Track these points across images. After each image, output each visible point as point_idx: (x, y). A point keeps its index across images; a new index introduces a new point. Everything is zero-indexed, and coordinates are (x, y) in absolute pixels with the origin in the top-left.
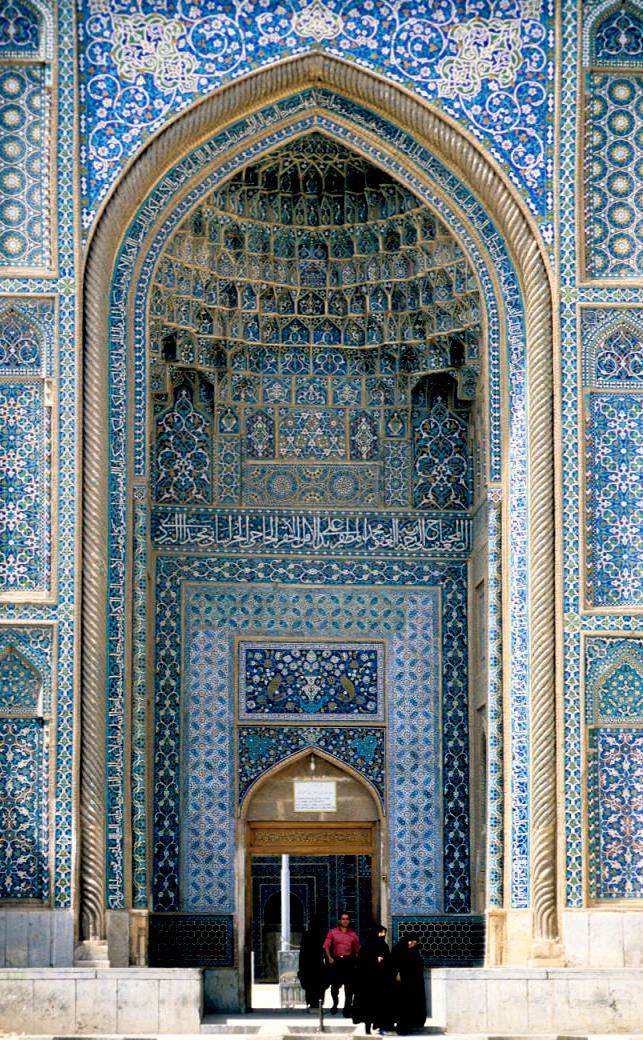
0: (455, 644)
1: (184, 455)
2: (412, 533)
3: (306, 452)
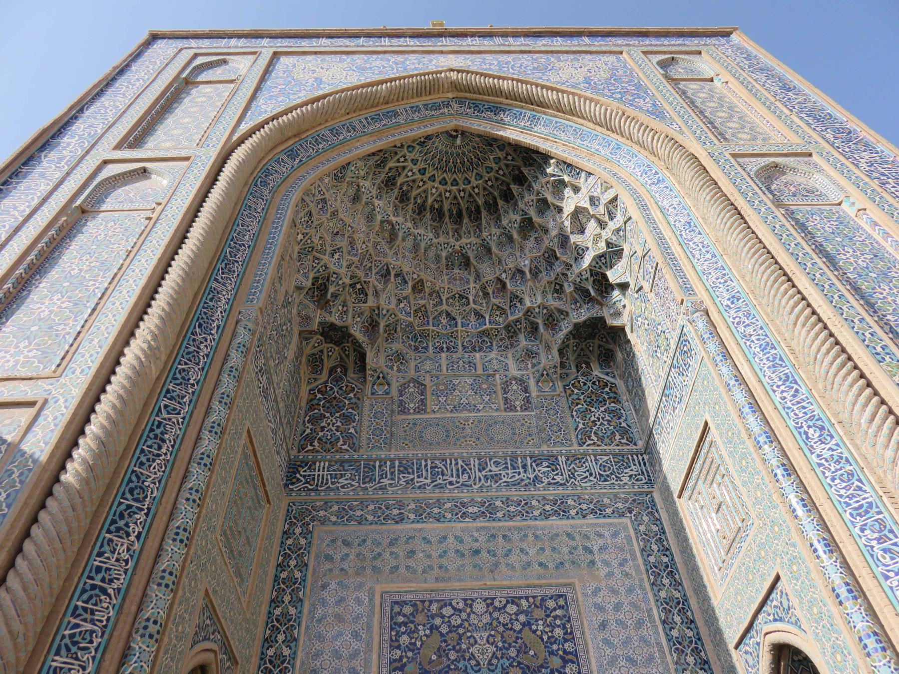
2: (583, 469)
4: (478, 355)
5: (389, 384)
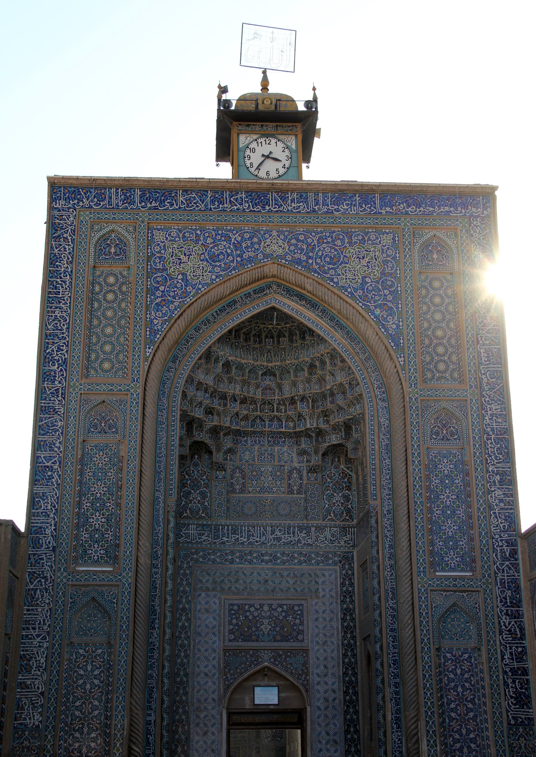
0: (348, 600)
1: (195, 491)
2: (322, 536)
3: (263, 490)
4: (276, 449)
5: (225, 471)
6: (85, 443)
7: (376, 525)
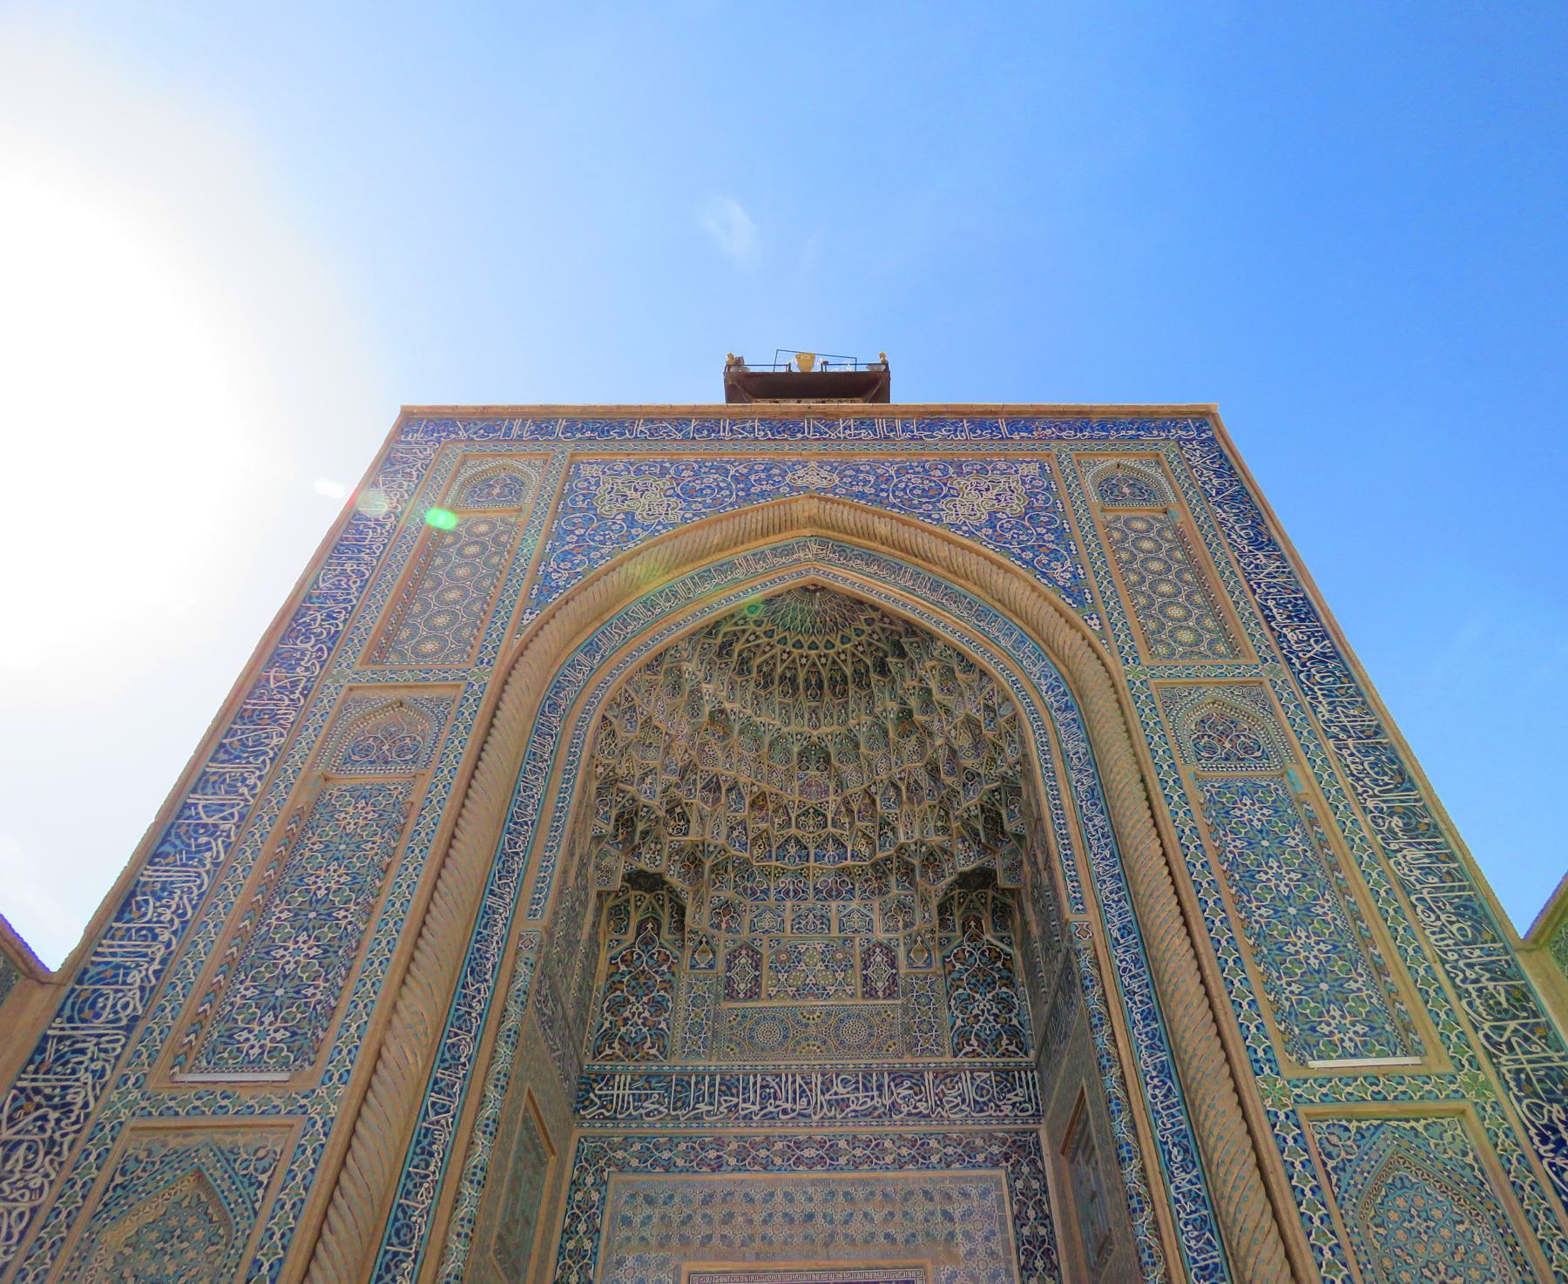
2: (954, 1093)
4: (834, 905)
6: (329, 784)
7: (1095, 972)
